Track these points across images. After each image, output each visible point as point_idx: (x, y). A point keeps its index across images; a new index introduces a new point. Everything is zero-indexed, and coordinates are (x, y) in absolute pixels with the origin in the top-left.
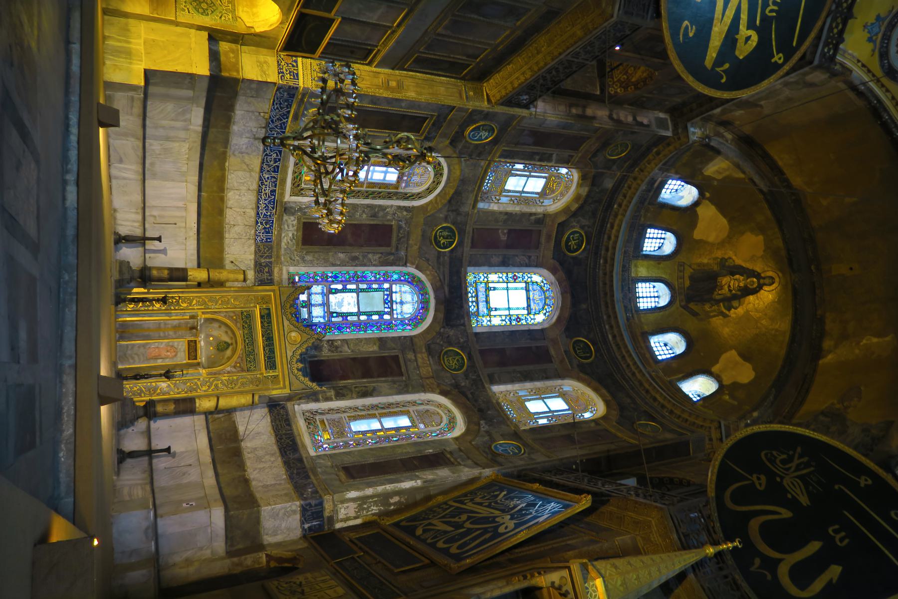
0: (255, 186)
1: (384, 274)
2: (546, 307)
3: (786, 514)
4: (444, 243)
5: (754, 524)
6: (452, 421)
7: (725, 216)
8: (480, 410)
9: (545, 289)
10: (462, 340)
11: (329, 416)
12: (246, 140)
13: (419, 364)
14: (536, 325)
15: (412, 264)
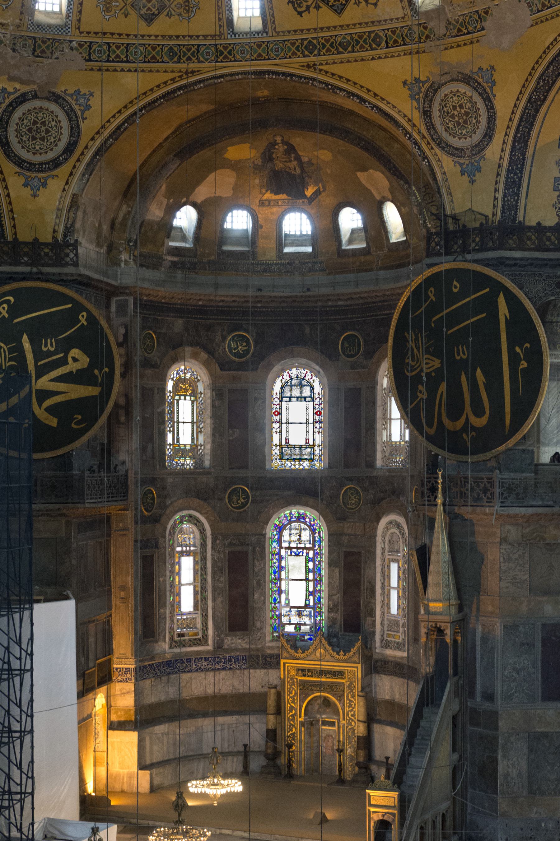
0: (202, 675)
1: (273, 555)
2: (307, 378)
3: (443, 387)
4: (244, 499)
5: (446, 421)
6: (398, 526)
7: (207, 177)
8: (394, 492)
9: (288, 378)
10: (335, 483)
11: (386, 629)
12: (170, 688)
13: (353, 533)
14: (324, 392)
15: (263, 528)
